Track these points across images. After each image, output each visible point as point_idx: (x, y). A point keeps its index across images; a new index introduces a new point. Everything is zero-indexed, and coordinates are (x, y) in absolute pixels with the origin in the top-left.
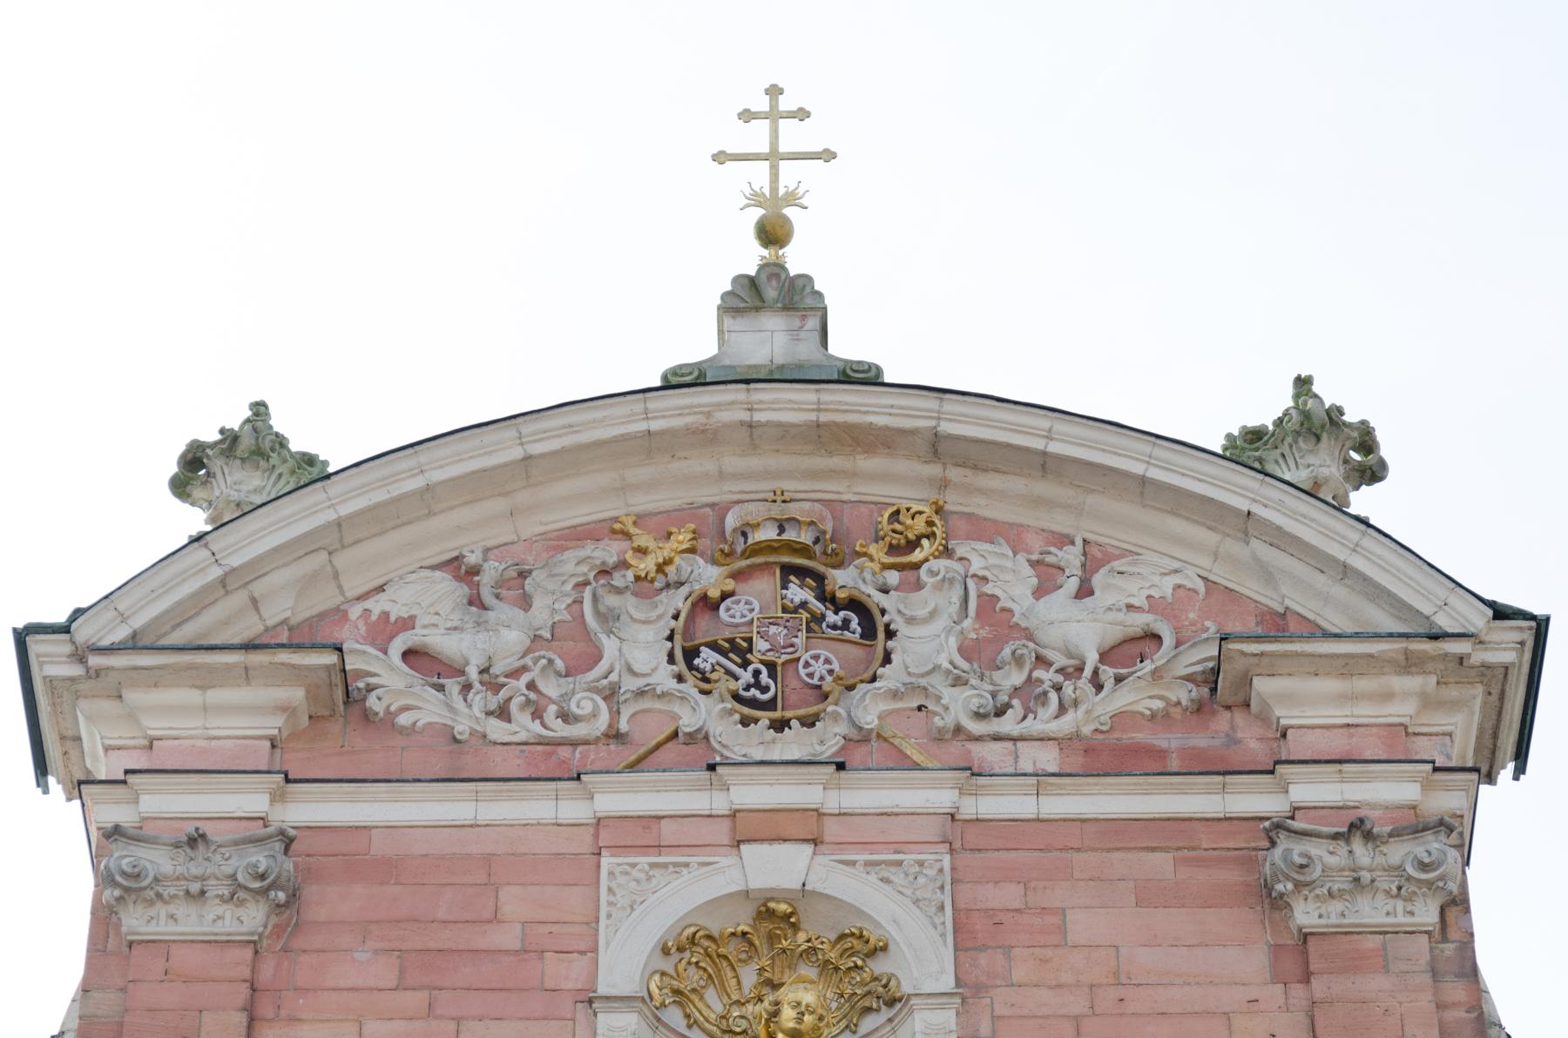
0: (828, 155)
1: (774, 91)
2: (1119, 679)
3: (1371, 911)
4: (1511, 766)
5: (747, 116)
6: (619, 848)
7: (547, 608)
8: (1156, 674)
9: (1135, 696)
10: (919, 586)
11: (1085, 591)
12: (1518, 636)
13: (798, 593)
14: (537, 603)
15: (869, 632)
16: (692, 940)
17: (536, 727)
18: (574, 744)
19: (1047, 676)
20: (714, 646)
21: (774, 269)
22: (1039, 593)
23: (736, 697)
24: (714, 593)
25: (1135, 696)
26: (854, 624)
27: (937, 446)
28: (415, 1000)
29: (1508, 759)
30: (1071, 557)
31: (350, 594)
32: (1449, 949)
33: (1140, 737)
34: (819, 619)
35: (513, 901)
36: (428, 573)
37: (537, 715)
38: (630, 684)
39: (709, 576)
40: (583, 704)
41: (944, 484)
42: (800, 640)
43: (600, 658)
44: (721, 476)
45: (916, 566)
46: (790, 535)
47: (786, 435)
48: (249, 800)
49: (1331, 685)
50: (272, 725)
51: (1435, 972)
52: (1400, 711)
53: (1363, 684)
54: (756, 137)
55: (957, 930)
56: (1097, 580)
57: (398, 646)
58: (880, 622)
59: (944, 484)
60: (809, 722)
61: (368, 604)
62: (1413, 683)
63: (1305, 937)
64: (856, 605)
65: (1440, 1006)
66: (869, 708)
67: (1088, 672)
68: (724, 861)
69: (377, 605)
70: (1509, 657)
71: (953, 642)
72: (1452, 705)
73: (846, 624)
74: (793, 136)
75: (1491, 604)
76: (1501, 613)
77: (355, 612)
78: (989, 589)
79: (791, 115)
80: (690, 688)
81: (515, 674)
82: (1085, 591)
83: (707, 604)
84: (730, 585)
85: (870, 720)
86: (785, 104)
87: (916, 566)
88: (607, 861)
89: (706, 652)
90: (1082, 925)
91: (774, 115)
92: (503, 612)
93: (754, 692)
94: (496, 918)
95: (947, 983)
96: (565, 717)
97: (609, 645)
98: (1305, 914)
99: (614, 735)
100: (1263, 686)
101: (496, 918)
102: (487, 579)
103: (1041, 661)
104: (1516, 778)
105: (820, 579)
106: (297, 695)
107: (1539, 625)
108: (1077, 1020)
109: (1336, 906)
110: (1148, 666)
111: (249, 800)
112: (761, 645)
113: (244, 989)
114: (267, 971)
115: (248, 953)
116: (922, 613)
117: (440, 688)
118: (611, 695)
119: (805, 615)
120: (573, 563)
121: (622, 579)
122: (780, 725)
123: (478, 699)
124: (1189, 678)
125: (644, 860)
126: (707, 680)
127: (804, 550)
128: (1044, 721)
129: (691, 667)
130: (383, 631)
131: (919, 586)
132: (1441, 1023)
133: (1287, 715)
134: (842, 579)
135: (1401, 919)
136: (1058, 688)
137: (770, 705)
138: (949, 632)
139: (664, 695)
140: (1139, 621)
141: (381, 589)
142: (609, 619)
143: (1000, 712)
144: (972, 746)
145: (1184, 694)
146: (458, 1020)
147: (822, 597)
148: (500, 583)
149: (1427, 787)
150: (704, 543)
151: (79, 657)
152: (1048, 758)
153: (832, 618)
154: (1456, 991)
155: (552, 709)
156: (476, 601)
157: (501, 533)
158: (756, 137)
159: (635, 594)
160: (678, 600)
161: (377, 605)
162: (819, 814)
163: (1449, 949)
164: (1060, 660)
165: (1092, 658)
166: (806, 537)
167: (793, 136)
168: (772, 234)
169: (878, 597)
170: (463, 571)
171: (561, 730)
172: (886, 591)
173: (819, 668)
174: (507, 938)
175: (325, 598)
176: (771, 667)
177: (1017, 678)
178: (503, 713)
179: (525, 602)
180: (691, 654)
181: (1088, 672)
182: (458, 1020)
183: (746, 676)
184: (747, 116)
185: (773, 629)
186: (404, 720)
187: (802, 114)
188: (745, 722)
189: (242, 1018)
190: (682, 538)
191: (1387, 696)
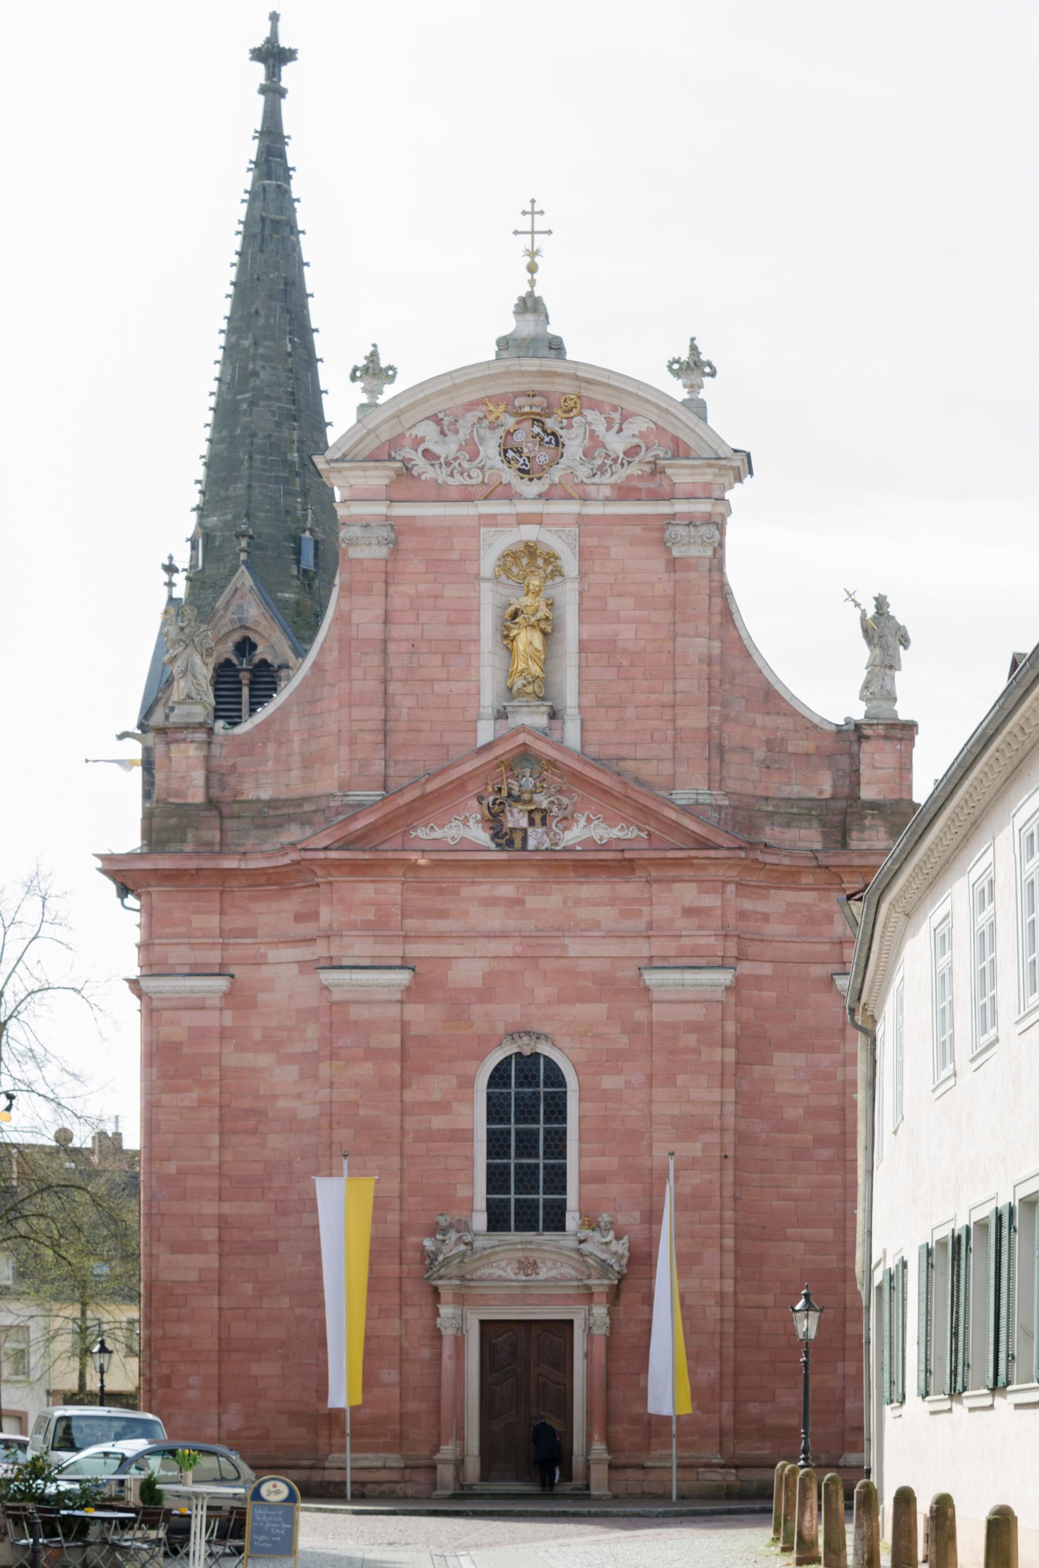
0: (550, 232)
1: (533, 201)
2: (629, 463)
3: (694, 551)
5: (524, 213)
6: (486, 525)
7: (463, 434)
8: (640, 462)
9: (633, 470)
10: (572, 427)
11: (620, 430)
13: (537, 430)
14: (461, 432)
15: (557, 445)
16: (507, 555)
17: (461, 479)
18: (472, 486)
19: (609, 462)
20: (512, 449)
21: (531, 294)
22: (608, 429)
23: (519, 470)
24: (512, 431)
25: (633, 470)
26: (553, 442)
27: (577, 378)
28: (431, 577)
30: (616, 416)
31: (406, 427)
32: (715, 561)
33: (634, 483)
34: (542, 440)
35: (458, 542)
36: (427, 421)
37: (462, 474)
38: (488, 465)
39: (510, 422)
40: (474, 473)
41: (580, 387)
42: (537, 448)
43: (478, 453)
44: (514, 384)
45: (572, 418)
46: (534, 410)
47: (532, 374)
48: (380, 509)
49: (688, 471)
50: (386, 481)
51: (710, 570)
52: (708, 478)
53: (697, 471)
54: (525, 223)
55: (580, 553)
56: (624, 426)
57: (420, 450)
58: (561, 440)
59: (580, 387)
60: (539, 478)
61: (411, 431)
62: (711, 470)
63: (675, 558)
64: (553, 434)
65: (711, 581)
66: (556, 474)
67: (619, 461)
68: (515, 530)
69: (414, 432)
71: (581, 450)
72: (724, 476)
73: (550, 443)
74: (541, 223)
77: (407, 434)
78: (593, 427)
79: (538, 213)
80: (505, 466)
81: (456, 459)
82: (620, 430)
83: (509, 434)
84: (516, 427)
85: (556, 480)
86: (537, 209)
87: (572, 418)
88: (483, 530)
89: (510, 452)
90: (615, 552)
91: (533, 213)
92: (451, 437)
93: (524, 467)
94: (452, 549)
95: (576, 573)
96: (469, 476)
97: (481, 449)
98: (676, 552)
99: (483, 482)
100: (668, 471)
101: (452, 549)
102: (446, 422)
103: (607, 456)
105: (543, 423)
106: (392, 473)
108: (611, 585)
109: (685, 548)
110: (637, 459)
111: (380, 509)
112: (525, 450)
113: (383, 576)
114: (390, 566)
115: (384, 563)
116: (573, 436)
117: (432, 465)
118: (482, 469)
119: (538, 439)
120: (471, 417)
121: (486, 423)
122: (531, 480)
123: (446, 470)
124: (649, 463)
125: (493, 529)
126: (509, 462)
127: (538, 414)
128: (607, 479)
129: (505, 456)
130: (418, 441)
131: (572, 427)
132: (710, 587)
133: (676, 480)
134: (550, 423)
135: (702, 554)
136: (611, 466)
137: (527, 472)
138: (579, 446)
139: (498, 469)
140: (637, 441)
141: (414, 426)
142: (482, 439)
143: (594, 475)
144: (587, 487)
145: (647, 469)
146: (443, 584)
147: (544, 431)
148: (450, 424)
149: (713, 505)
150: (510, 407)
151: (328, 462)
152: (607, 492)
153: (547, 439)
154: (716, 576)
155: (466, 474)
156: (443, 433)
157: (450, 404)
158: (525, 223)
159: (490, 428)
160: (501, 432)
161: (414, 432)
162: (542, 514)
163: (715, 561)
164: (614, 456)
165: (621, 455)
166: (538, 410)
167: (541, 223)
168: (532, 269)
169: (560, 432)
170: (438, 422)
171: (468, 481)
172: (562, 428)
173: (542, 459)
174: (455, 555)
175: (398, 431)
176: (528, 458)
177: (599, 462)
178: (452, 475)
179: (456, 432)
180: (505, 451)
181: (619, 461)
182: (443, 584)
183: (521, 461)
184: (524, 213)
185: (529, 445)
186: (423, 477)
187: (542, 213)
188: (522, 478)
189: (383, 585)
190: (502, 407)
191: (704, 474)
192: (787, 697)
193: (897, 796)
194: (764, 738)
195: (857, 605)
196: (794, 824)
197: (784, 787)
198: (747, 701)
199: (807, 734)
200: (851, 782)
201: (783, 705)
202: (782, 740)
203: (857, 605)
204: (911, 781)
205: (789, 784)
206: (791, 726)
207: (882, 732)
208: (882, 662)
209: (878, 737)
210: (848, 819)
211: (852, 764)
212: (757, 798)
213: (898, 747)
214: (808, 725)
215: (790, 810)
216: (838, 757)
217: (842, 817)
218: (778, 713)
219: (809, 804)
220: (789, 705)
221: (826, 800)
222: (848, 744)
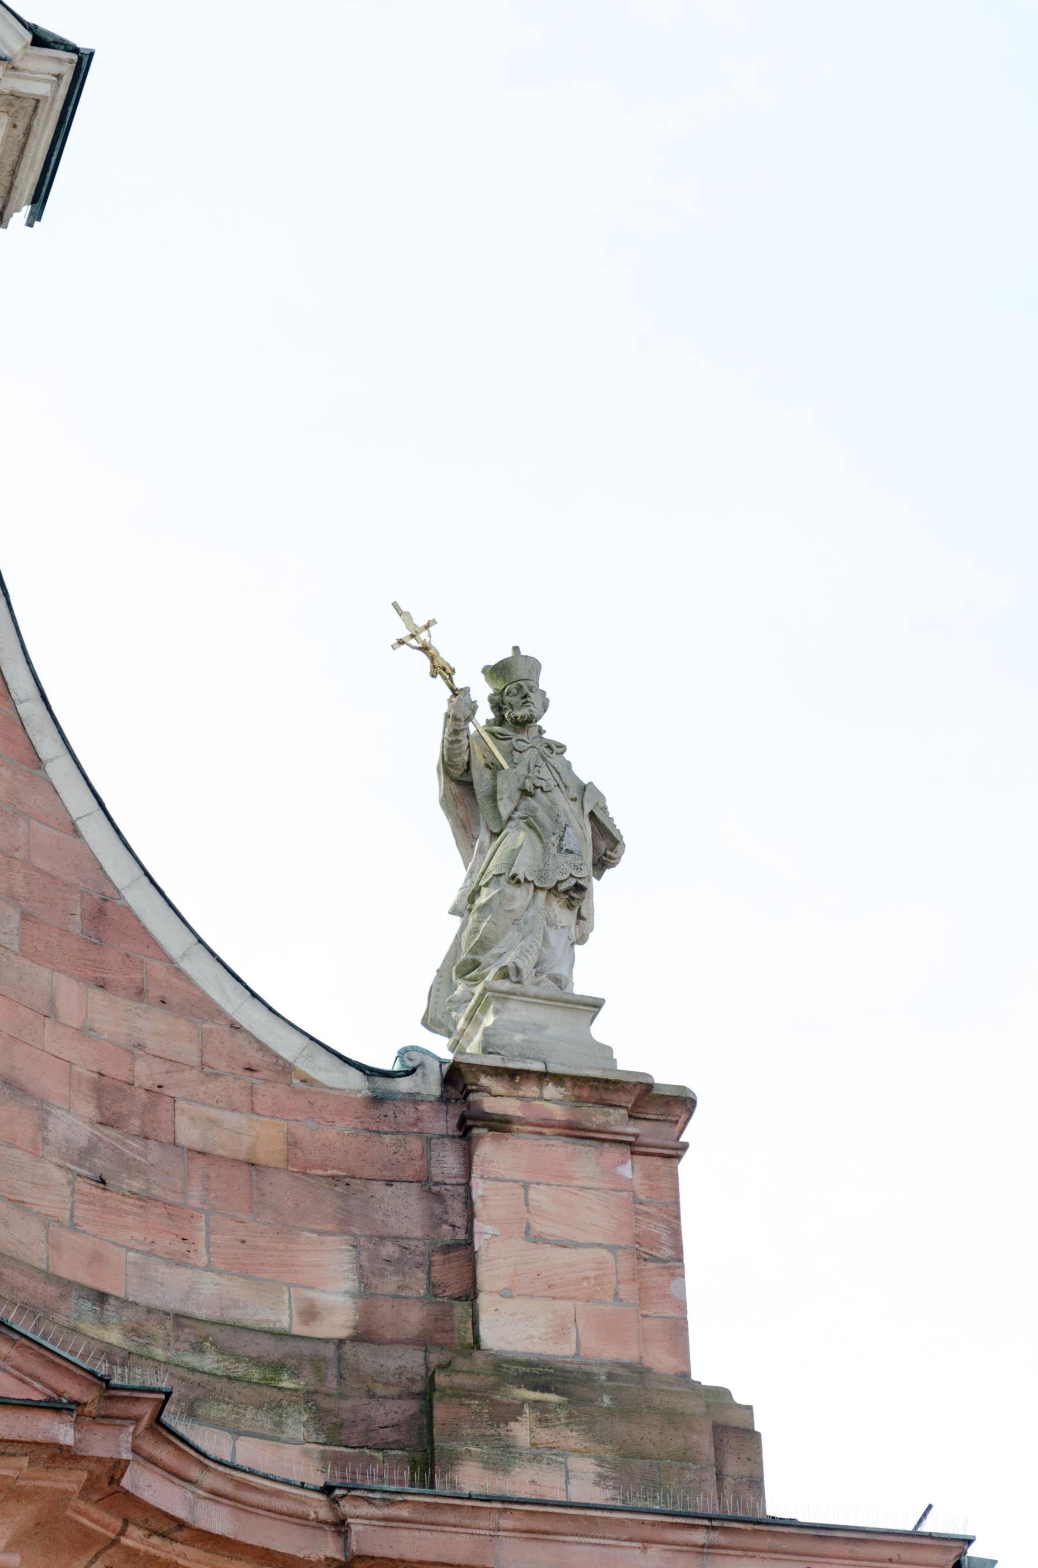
4: (26, 209)
12: (56, 68)
29: (24, 201)
70: (41, 89)
75: (32, 28)
76: (40, 39)
104: (30, 224)
107: (80, 59)
192: (172, 941)
193: (629, 1354)
194: (85, 1071)
195: (441, 670)
196: (215, 1412)
197: (162, 1271)
198: (25, 917)
199: (252, 1091)
200: (432, 1286)
201: (158, 969)
202: (156, 1091)
203: (441, 670)
204: (682, 1307)
205: (180, 1261)
206: (189, 1052)
207: (559, 1113)
208: (542, 875)
209: (542, 1126)
210: (440, 1412)
211: (437, 1221)
212: (67, 1285)
213: (626, 1170)
214: (256, 1058)
215: (192, 1360)
216: (379, 1189)
217: (411, 1407)
218: (140, 993)
219: (266, 1347)
220: (179, 972)
221: (341, 1342)
222: (415, 1145)
